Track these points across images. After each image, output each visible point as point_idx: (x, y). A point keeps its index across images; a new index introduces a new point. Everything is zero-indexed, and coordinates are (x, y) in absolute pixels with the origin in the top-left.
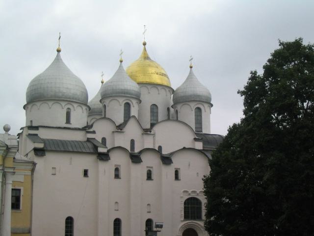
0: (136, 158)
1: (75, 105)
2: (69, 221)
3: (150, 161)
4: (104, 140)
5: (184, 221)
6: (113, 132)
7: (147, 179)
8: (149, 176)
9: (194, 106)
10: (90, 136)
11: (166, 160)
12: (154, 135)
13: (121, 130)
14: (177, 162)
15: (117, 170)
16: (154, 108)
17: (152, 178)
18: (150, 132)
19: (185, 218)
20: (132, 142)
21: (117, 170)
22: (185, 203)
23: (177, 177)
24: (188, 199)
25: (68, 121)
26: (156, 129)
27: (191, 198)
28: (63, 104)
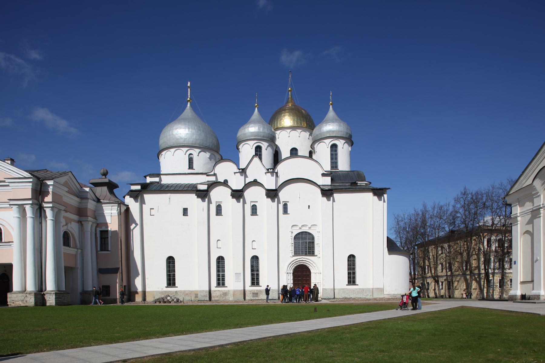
2: (171, 261)
5: (293, 256)
6: (235, 173)
7: (251, 215)
9: (328, 142)
11: (272, 194)
12: (277, 173)
13: (240, 170)
14: (283, 195)
17: (258, 214)
18: (271, 170)
19: (294, 254)
22: (295, 238)
24: (299, 234)
25: (191, 166)
26: (280, 168)
27: (302, 233)
28: (185, 149)
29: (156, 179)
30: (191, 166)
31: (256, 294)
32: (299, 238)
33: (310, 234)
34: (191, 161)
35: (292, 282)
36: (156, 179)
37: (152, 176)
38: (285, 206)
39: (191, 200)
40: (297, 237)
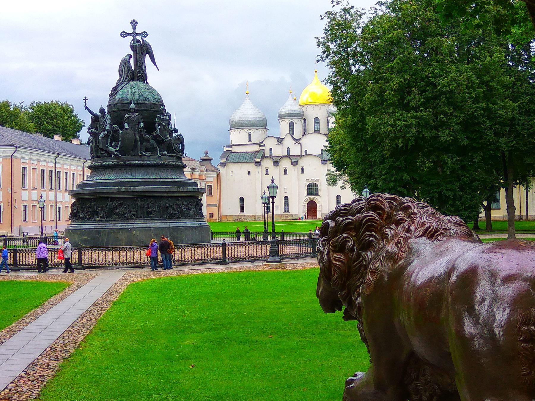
0: (276, 164)
1: (254, 130)
2: (242, 199)
3: (286, 163)
4: (271, 149)
8: (286, 173)
10: (262, 148)
11: (295, 163)
12: (301, 144)
15: (267, 170)
16: (317, 120)
20: (288, 149)
21: (267, 170)
23: (303, 172)
25: (250, 140)
28: (246, 130)
29: (230, 149)
30: (250, 140)
31: (286, 217)
32: (310, 187)
33: (316, 184)
34: (250, 136)
35: (307, 210)
36: (230, 149)
37: (227, 146)
38: (302, 169)
39: (251, 167)
40: (309, 186)
